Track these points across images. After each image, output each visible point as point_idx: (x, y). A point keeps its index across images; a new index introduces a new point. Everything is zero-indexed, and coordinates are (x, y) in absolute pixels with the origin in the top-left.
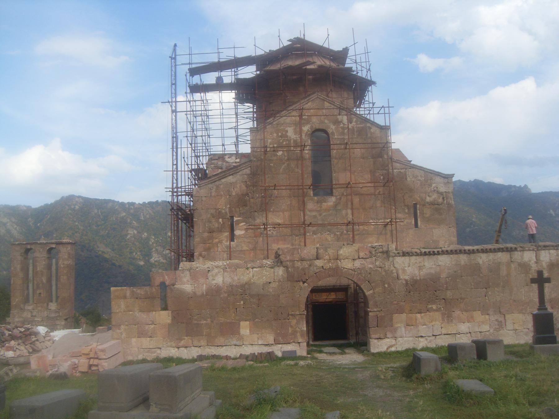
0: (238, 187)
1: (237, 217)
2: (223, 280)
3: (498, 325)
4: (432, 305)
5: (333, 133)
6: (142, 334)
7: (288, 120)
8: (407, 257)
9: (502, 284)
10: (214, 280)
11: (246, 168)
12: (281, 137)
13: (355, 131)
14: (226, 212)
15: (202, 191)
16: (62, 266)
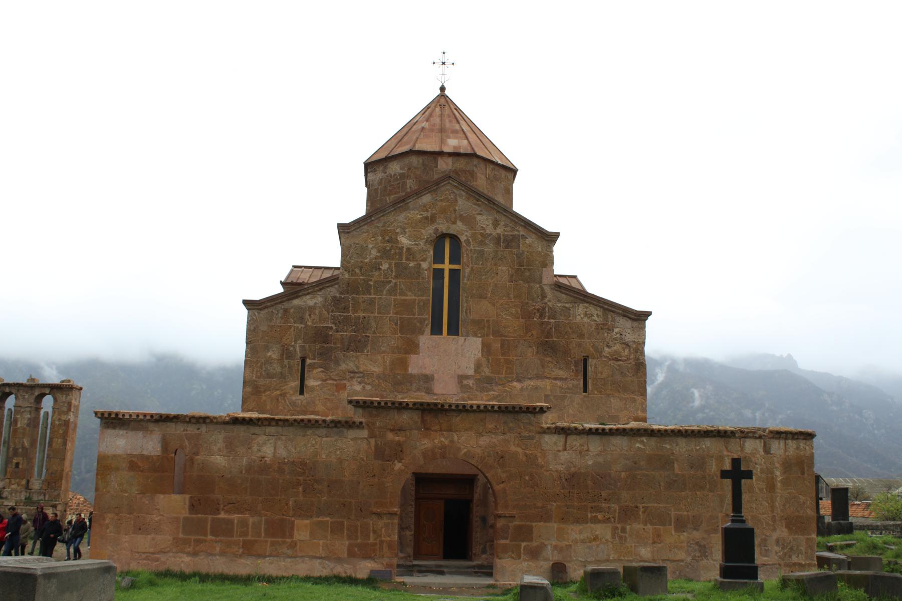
0: (317, 314)
1: (312, 360)
2: (274, 453)
3: (700, 551)
4: (597, 513)
5: (468, 242)
6: (140, 529)
7: (402, 217)
8: (561, 436)
9: (708, 486)
10: (259, 450)
11: (331, 286)
12: (388, 241)
13: (502, 241)
15: (261, 315)
16: (57, 423)
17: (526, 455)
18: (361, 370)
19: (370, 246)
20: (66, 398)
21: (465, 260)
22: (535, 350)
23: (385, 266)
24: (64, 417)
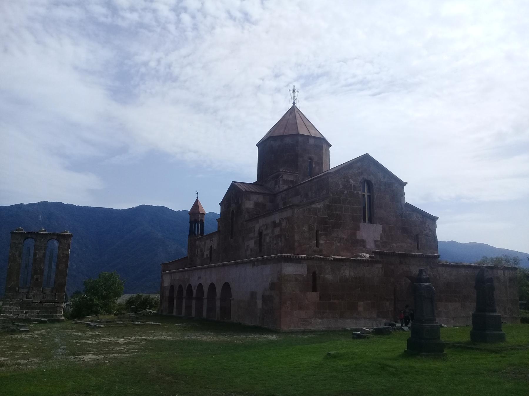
2: (349, 274)
10: (344, 272)
14: (314, 227)
17: (433, 275)
18: (339, 237)
19: (340, 183)
20: (67, 241)
21: (374, 191)
22: (400, 231)
23: (345, 192)
24: (65, 253)
